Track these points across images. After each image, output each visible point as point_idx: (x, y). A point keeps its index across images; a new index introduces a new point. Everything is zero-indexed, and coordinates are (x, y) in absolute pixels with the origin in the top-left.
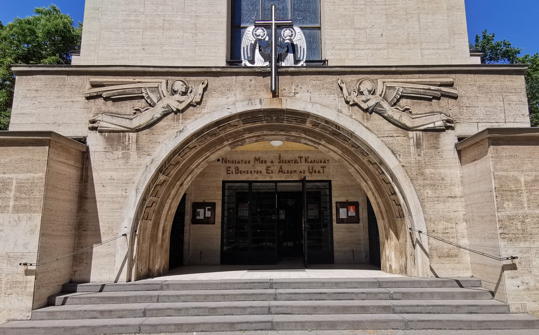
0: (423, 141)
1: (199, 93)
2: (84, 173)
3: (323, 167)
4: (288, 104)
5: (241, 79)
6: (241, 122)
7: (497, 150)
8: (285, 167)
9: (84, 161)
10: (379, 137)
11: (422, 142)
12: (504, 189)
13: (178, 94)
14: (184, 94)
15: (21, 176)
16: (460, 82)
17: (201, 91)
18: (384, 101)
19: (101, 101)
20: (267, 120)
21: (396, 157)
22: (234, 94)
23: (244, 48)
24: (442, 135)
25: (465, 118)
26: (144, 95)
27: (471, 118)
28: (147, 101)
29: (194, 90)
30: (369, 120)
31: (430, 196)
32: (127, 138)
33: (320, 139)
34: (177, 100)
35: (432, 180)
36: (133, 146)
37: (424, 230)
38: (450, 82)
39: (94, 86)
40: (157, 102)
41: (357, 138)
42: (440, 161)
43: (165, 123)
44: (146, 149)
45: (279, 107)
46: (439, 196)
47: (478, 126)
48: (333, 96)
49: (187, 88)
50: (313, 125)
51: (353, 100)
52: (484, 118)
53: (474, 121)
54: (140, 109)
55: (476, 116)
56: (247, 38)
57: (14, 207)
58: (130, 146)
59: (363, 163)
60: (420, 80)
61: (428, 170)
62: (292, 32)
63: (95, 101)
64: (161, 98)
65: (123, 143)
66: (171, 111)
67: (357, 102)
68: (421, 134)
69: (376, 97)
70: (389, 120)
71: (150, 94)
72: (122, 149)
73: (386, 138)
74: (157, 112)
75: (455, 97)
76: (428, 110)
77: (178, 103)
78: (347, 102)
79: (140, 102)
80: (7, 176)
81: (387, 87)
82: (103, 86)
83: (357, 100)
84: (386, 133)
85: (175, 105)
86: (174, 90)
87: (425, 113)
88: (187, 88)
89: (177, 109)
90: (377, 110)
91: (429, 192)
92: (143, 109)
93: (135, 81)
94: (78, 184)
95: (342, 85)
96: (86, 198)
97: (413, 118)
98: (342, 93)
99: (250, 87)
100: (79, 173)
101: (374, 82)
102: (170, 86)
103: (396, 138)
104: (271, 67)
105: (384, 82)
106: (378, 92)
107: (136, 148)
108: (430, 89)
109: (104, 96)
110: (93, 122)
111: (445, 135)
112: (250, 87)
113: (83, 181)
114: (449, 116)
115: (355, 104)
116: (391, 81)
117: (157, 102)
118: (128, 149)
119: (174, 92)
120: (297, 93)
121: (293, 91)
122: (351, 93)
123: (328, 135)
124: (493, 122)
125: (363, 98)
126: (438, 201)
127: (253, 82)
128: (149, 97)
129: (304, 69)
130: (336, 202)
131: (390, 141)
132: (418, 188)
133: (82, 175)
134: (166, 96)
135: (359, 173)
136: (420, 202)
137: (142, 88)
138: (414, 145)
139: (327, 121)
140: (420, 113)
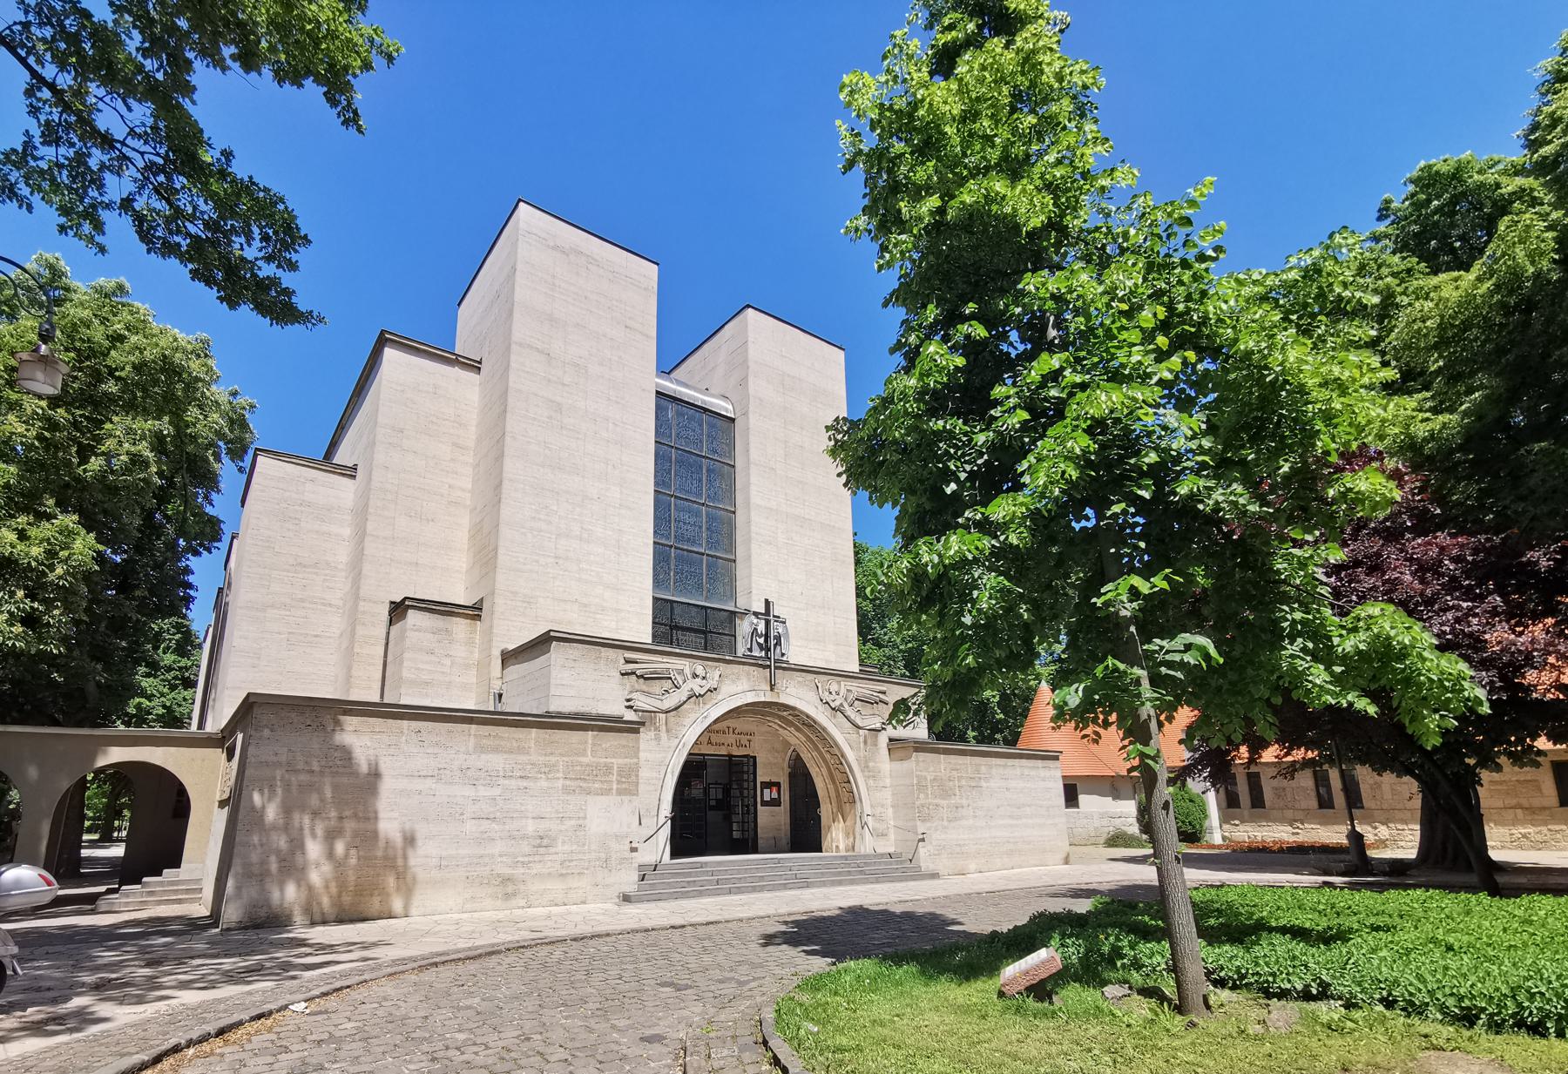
4: (783, 700)
8: (714, 738)
15: (620, 761)
17: (717, 678)
19: (634, 677)
36: (663, 728)
39: (628, 661)
74: (682, 694)
80: (609, 760)
85: (698, 691)
91: (871, 782)
110: (628, 700)
119: (695, 676)
125: (832, 697)
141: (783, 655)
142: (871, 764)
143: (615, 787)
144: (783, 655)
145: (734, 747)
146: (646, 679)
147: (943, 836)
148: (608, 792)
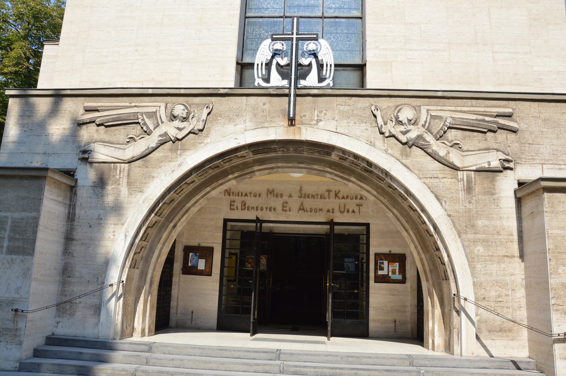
0: (475, 184)
1: (202, 119)
2: (71, 211)
5: (252, 102)
6: (251, 153)
7: (552, 203)
9: (72, 197)
10: (420, 178)
11: (473, 186)
12: (560, 251)
13: (178, 120)
14: (185, 119)
16: (521, 113)
17: (204, 116)
18: (428, 133)
20: (283, 151)
21: (441, 204)
22: (244, 120)
23: (258, 65)
24: (499, 177)
25: (527, 157)
26: (140, 121)
27: (534, 158)
28: (142, 128)
29: (196, 115)
30: (409, 156)
31: (481, 254)
32: (118, 171)
33: (350, 175)
34: (177, 127)
35: (485, 234)
36: (124, 181)
37: (472, 297)
38: (509, 112)
40: (154, 129)
41: (392, 178)
42: (496, 210)
43: (161, 154)
44: (138, 184)
45: (297, 138)
46: (493, 254)
47: (542, 168)
48: (364, 124)
49: (188, 114)
50: (340, 159)
51: (389, 131)
52: (551, 158)
53: (538, 162)
54: (135, 137)
55: (541, 155)
56: (263, 53)
58: (121, 180)
59: (403, 208)
60: (472, 109)
61: (480, 222)
62: (317, 45)
63: (87, 128)
64: (158, 125)
65: (114, 176)
66: (168, 140)
67: (394, 133)
68: (473, 176)
69: (418, 128)
70: (434, 156)
71: (146, 119)
72: (112, 184)
73: (429, 179)
74: (153, 140)
75: (514, 131)
76: (482, 145)
77: (177, 131)
78: (382, 133)
79: (134, 129)
82: (98, 111)
83: (393, 132)
84: (429, 173)
85: (173, 133)
86: (173, 116)
87: (479, 150)
88: (188, 114)
89: (176, 138)
90: (419, 144)
91: (480, 249)
92: (137, 137)
93: (132, 105)
94: (65, 223)
95: (375, 112)
96: (72, 239)
97: (463, 156)
98: (376, 122)
99: (263, 112)
100: (67, 211)
101: (417, 109)
102: (169, 111)
103: (442, 180)
104: (289, 88)
105: (428, 110)
106: (422, 122)
107: (127, 182)
108: (484, 121)
109: (98, 123)
111: (503, 177)
112: (263, 112)
113: (70, 219)
114: (508, 155)
116: (437, 109)
117: (154, 129)
118: (119, 184)
119: (173, 117)
120: (321, 120)
121: (316, 118)
122: (387, 121)
123: (359, 170)
124: (561, 163)
125: (402, 128)
126: (491, 260)
127: (267, 106)
128: (145, 124)
129: (330, 92)
130: (376, 255)
131: (434, 184)
132: (466, 243)
133: (69, 213)
134: (164, 122)
135: (399, 220)
136: (468, 261)
137: (138, 112)
138: (464, 190)
139: (356, 157)
140: (472, 149)
142: (480, 223)
145: (337, 214)
146: (106, 126)
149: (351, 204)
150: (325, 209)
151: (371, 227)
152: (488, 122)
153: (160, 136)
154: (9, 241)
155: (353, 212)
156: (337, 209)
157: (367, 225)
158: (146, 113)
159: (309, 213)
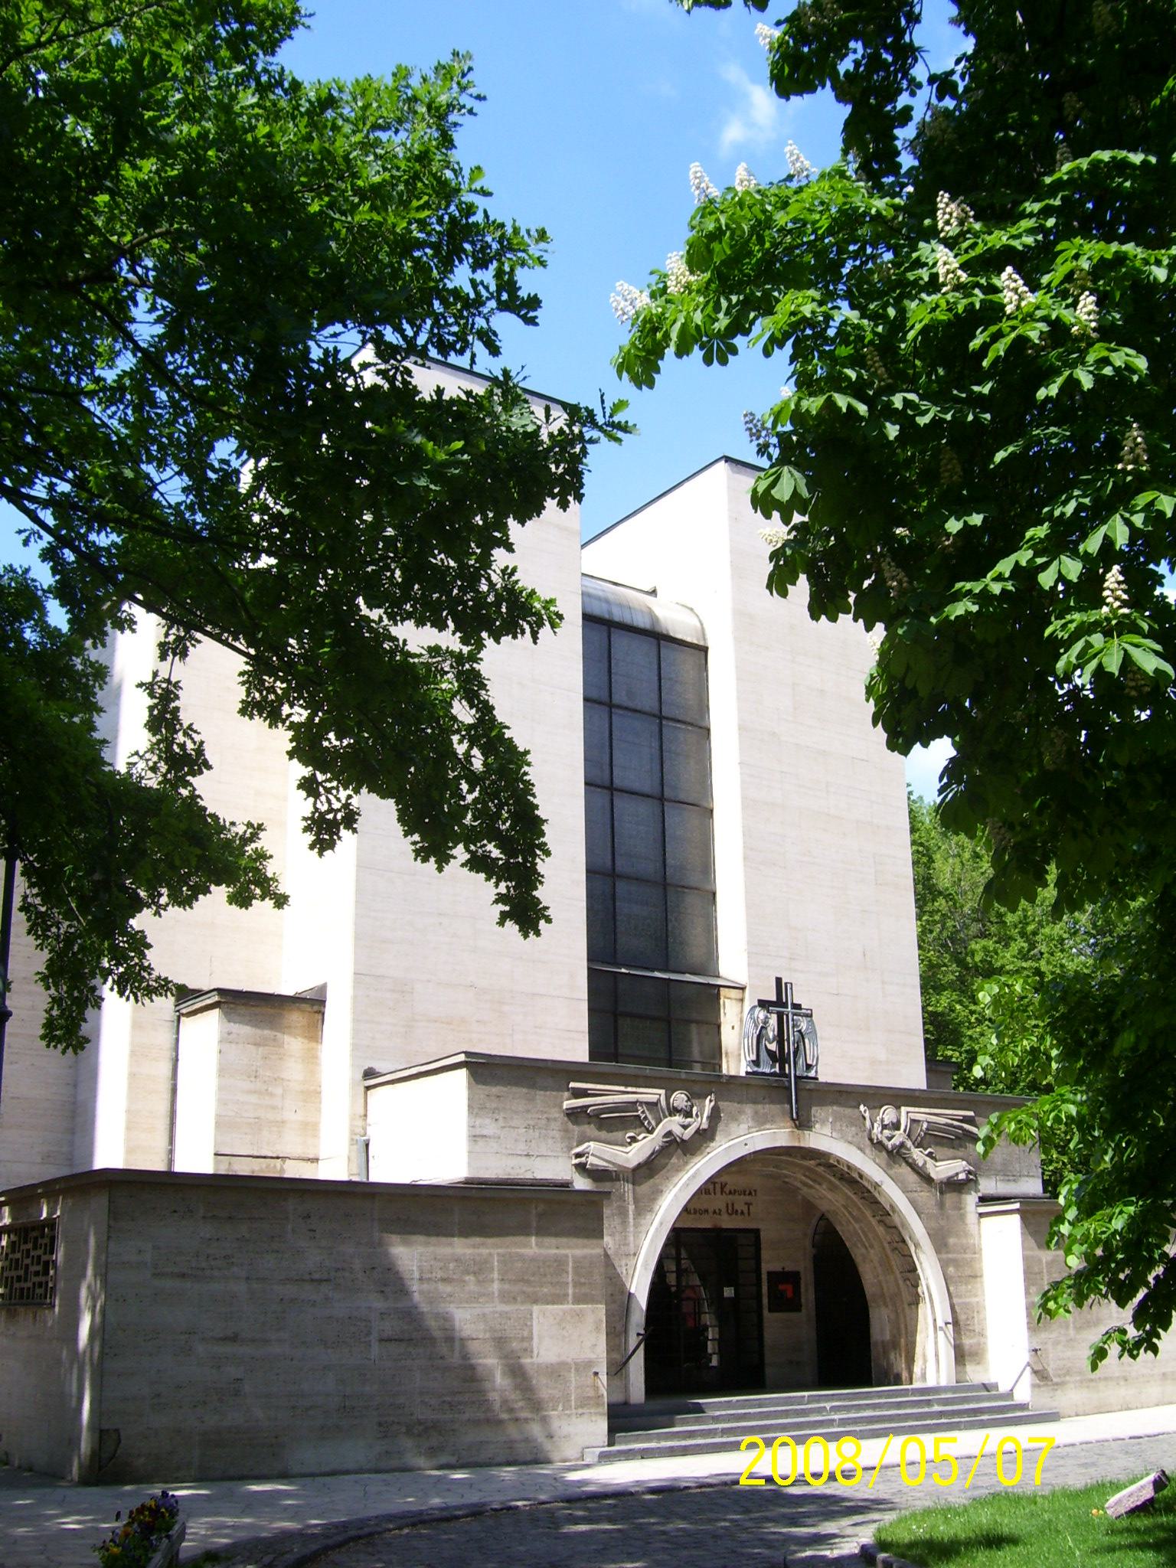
3: (748, 1204)
14: (688, 1114)
45: (802, 1145)
57: (574, 1294)
81: (913, 1121)
106: (903, 1127)
110: (578, 1155)
115: (880, 1143)
119: (674, 1111)
128: (646, 1118)
130: (769, 1273)
141: (809, 1067)
143: (570, 1291)
144: (809, 1067)
145: (725, 1216)
147: (1069, 1354)
148: (558, 1299)
149: (740, 1202)
150: (711, 1210)
151: (762, 1234)
152: (955, 1127)
153: (665, 1136)
154: (575, 1286)
155: (742, 1213)
156: (724, 1210)
157: (757, 1232)
158: (647, 1104)
159: (692, 1216)
